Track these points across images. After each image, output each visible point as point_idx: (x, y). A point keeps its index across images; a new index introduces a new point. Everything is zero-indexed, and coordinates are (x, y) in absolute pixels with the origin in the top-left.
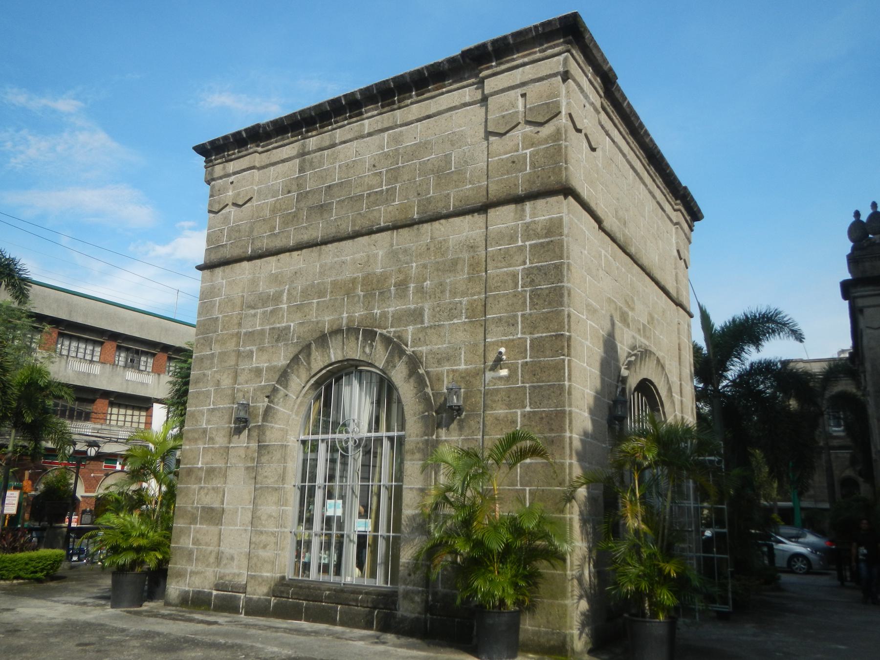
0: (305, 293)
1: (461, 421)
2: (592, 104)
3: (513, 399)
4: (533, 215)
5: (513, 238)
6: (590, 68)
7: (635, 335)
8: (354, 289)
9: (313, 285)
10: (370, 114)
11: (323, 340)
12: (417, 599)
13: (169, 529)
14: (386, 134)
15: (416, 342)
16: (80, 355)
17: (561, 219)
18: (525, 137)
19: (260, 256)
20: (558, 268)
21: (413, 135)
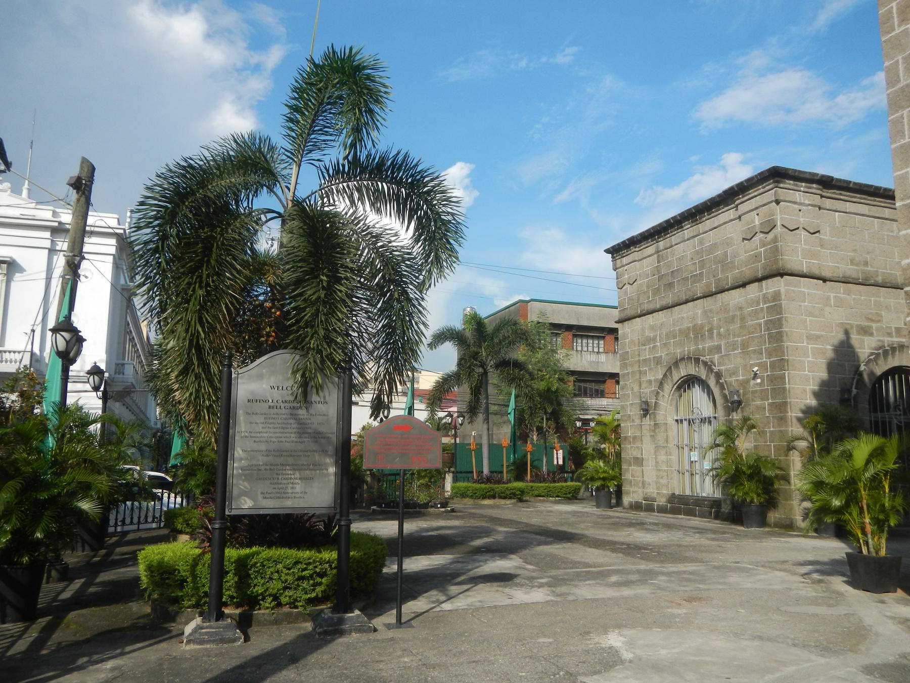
0: (668, 336)
1: (742, 408)
2: (809, 205)
3: (763, 395)
4: (767, 289)
5: (758, 304)
6: (804, 184)
7: (882, 339)
8: (689, 333)
9: (670, 332)
10: (686, 227)
11: (676, 364)
12: (728, 502)
13: (620, 469)
14: (696, 239)
15: (720, 364)
16: (590, 349)
17: (779, 291)
18: (761, 241)
19: (644, 315)
20: (780, 320)
21: (711, 238)
